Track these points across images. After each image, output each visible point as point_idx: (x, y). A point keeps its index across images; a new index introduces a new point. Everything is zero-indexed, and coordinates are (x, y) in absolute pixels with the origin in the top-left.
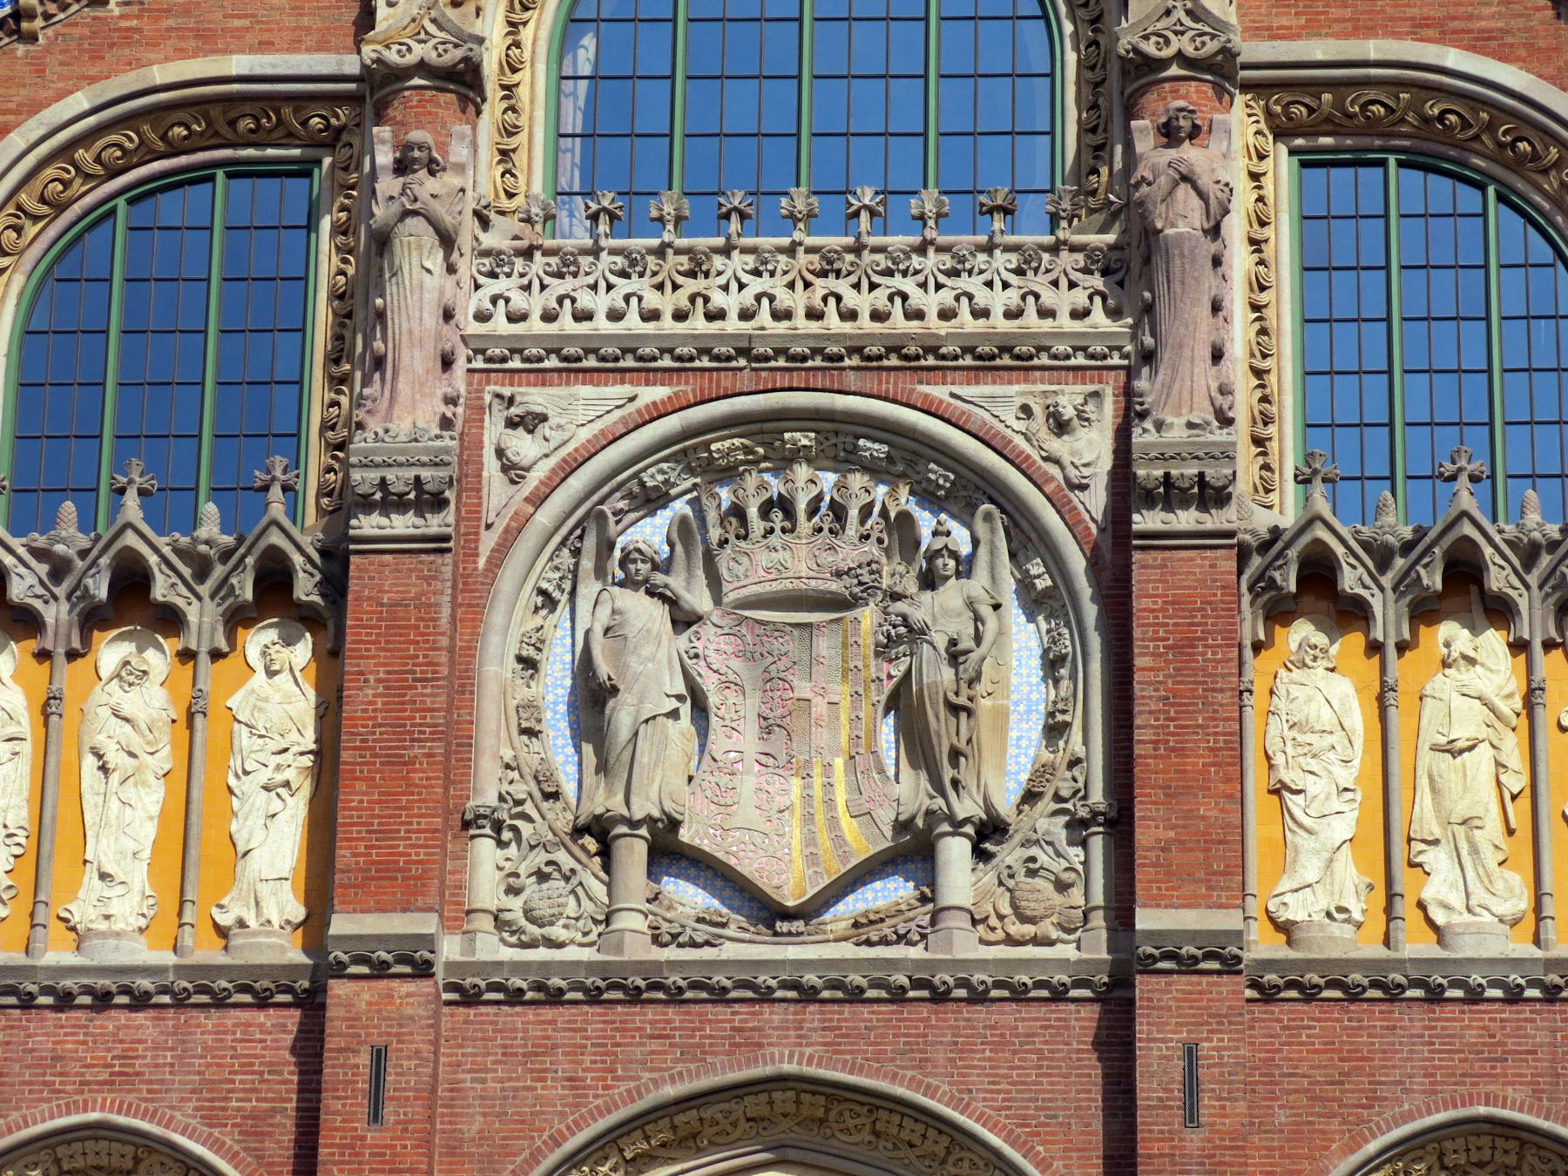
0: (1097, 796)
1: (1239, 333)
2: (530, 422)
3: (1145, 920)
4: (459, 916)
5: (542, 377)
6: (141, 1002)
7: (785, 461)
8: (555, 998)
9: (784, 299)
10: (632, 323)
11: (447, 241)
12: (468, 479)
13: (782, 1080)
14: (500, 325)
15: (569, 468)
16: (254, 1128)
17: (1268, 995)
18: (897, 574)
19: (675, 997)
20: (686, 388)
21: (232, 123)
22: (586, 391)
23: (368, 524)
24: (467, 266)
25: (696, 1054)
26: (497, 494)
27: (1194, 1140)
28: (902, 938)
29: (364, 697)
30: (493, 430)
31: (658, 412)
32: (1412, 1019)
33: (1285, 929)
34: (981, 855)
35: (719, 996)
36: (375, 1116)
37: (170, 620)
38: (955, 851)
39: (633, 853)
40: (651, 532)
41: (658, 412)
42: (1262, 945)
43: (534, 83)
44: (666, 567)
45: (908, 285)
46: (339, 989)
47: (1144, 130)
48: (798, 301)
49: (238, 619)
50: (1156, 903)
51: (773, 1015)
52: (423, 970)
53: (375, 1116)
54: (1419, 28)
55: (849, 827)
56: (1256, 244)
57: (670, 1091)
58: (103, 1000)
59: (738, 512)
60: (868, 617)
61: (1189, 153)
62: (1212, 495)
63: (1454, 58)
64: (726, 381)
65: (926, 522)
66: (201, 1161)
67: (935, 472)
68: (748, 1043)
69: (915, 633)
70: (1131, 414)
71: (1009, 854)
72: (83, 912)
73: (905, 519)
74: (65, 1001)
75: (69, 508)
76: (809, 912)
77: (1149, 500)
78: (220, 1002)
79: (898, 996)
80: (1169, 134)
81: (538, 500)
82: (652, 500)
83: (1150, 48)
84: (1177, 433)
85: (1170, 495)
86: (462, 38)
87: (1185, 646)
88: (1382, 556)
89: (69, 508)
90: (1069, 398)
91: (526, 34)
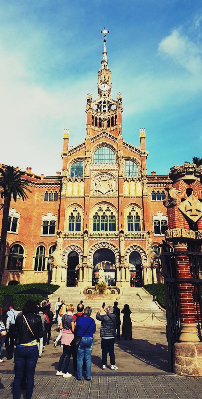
0: (117, 189)
1: (123, 169)
3: (119, 195)
4: (90, 194)
6: (77, 198)
7: (104, 174)
8: (94, 198)
10: (97, 168)
11: (89, 165)
12: (90, 175)
14: (91, 168)
15: (95, 175)
16: (82, 203)
17: (124, 198)
18: (109, 179)
19: (99, 198)
20: (99, 171)
23: (86, 177)
24: (90, 166)
25: (100, 200)
26: (91, 176)
27: (121, 204)
29: (86, 185)
30: (91, 173)
31: (98, 172)
32: (130, 199)
33: (125, 195)
35: (101, 198)
36: (87, 203)
37: (78, 181)
38: (111, 191)
39: (97, 191)
40: (98, 177)
41: (98, 172)
42: (124, 196)
43: (92, 157)
44: (98, 179)
46: (85, 198)
47: (119, 160)
48: (104, 167)
51: (103, 199)
52: (89, 197)
53: (87, 203)
54: (131, 155)
58: (75, 198)
59: (102, 177)
60: (107, 181)
61: (121, 161)
62: (122, 176)
63: (132, 157)
65: (110, 177)
68: (102, 200)
69: (109, 182)
70: (118, 173)
71: (113, 192)
72: (74, 194)
73: (109, 177)
74: (74, 198)
75: (73, 177)
76: (105, 194)
77: (119, 176)
78: (80, 198)
79: (109, 198)
80: (120, 160)
82: (98, 176)
84: (120, 174)
85: (120, 176)
87: (121, 183)
88: (129, 179)
89: (73, 177)
90: (116, 172)
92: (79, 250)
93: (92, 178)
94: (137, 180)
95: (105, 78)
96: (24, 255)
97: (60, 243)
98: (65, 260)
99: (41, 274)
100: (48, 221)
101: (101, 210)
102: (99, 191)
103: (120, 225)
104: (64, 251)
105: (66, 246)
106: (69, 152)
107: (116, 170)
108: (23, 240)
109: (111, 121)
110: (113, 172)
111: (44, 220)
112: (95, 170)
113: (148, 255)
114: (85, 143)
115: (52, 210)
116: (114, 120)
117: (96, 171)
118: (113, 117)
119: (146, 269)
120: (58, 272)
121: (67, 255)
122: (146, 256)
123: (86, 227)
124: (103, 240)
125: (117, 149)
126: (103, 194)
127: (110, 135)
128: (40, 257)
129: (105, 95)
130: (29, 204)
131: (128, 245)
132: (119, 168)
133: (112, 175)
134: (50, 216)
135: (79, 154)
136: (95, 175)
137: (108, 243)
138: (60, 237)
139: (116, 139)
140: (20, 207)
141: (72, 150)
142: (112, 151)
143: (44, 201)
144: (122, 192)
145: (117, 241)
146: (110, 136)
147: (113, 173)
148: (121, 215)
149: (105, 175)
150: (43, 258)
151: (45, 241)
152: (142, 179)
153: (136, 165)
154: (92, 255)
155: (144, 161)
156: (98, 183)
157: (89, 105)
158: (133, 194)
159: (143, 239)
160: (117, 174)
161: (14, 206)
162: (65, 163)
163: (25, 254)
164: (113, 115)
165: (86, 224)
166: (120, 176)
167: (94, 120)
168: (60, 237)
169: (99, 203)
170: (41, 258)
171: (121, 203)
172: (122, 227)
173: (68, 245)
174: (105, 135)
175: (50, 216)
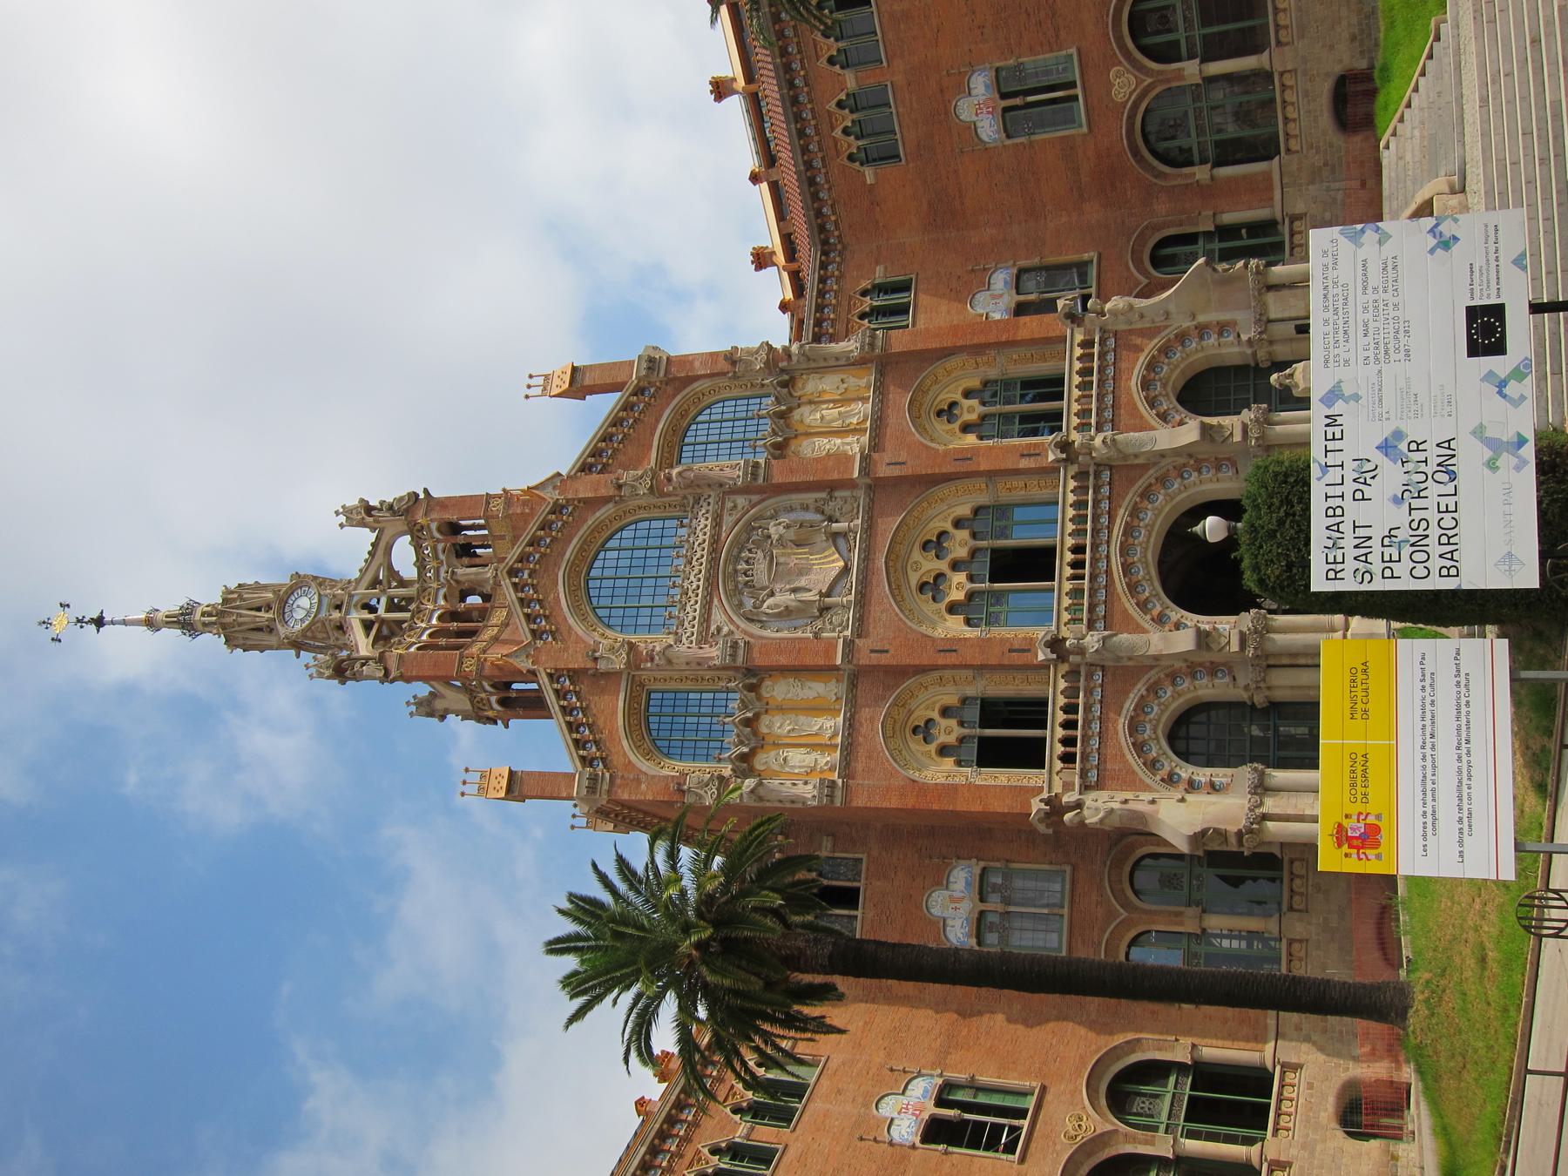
0: (824, 495)
2: (719, 630)
5: (708, 627)
9: (696, 571)
10: (697, 607)
22: (713, 617)
27: (909, 463)
28: (855, 538)
34: (837, 522)
36: (887, 651)
40: (749, 603)
45: (697, 544)
49: (759, 698)
50: (852, 473)
53: (887, 651)
57: (887, 588)
63: (660, 426)
64: (715, 584)
67: (743, 537)
72: (829, 733)
81: (738, 627)
83: (648, 486)
86: (623, 645)
90: (729, 505)
92: (1161, 693)
94: (785, 391)
95: (259, 609)
97: (1116, 806)
98: (1217, 776)
99: (1302, 954)
101: (933, 586)
102: (828, 594)
103: (1024, 463)
104: (1163, 780)
105: (1134, 772)
106: (584, 766)
107: (722, 501)
108: (1081, 1057)
110: (728, 520)
111: (973, 942)
112: (706, 618)
113: (1194, 316)
114: (550, 676)
117: (714, 610)
119: (1270, 321)
120: (1290, 811)
121: (1186, 771)
122: (1202, 330)
124: (1108, 557)
125: (611, 505)
126: (846, 570)
127: (530, 544)
129: (338, 607)
131: (1142, 417)
132: (709, 486)
133: (749, 529)
134: (953, 900)
136: (735, 618)
137: (1129, 531)
138: (1079, 805)
139: (557, 509)
140: (874, 1070)
142: (618, 536)
144: (843, 459)
145: (1116, 477)
146: (535, 542)
147: (734, 518)
149: (742, 566)
152: (783, 371)
153: (708, 411)
154: (1192, 619)
155: (691, 363)
156: (783, 599)
157: (363, 665)
158: (861, 411)
159: (1111, 343)
160: (741, 501)
161: (860, 1100)
162: (643, 786)
166: (755, 476)
167: (443, 641)
168: (1079, 805)
169: (896, 592)
172: (1039, 455)
173: (1129, 757)
175: (953, 900)
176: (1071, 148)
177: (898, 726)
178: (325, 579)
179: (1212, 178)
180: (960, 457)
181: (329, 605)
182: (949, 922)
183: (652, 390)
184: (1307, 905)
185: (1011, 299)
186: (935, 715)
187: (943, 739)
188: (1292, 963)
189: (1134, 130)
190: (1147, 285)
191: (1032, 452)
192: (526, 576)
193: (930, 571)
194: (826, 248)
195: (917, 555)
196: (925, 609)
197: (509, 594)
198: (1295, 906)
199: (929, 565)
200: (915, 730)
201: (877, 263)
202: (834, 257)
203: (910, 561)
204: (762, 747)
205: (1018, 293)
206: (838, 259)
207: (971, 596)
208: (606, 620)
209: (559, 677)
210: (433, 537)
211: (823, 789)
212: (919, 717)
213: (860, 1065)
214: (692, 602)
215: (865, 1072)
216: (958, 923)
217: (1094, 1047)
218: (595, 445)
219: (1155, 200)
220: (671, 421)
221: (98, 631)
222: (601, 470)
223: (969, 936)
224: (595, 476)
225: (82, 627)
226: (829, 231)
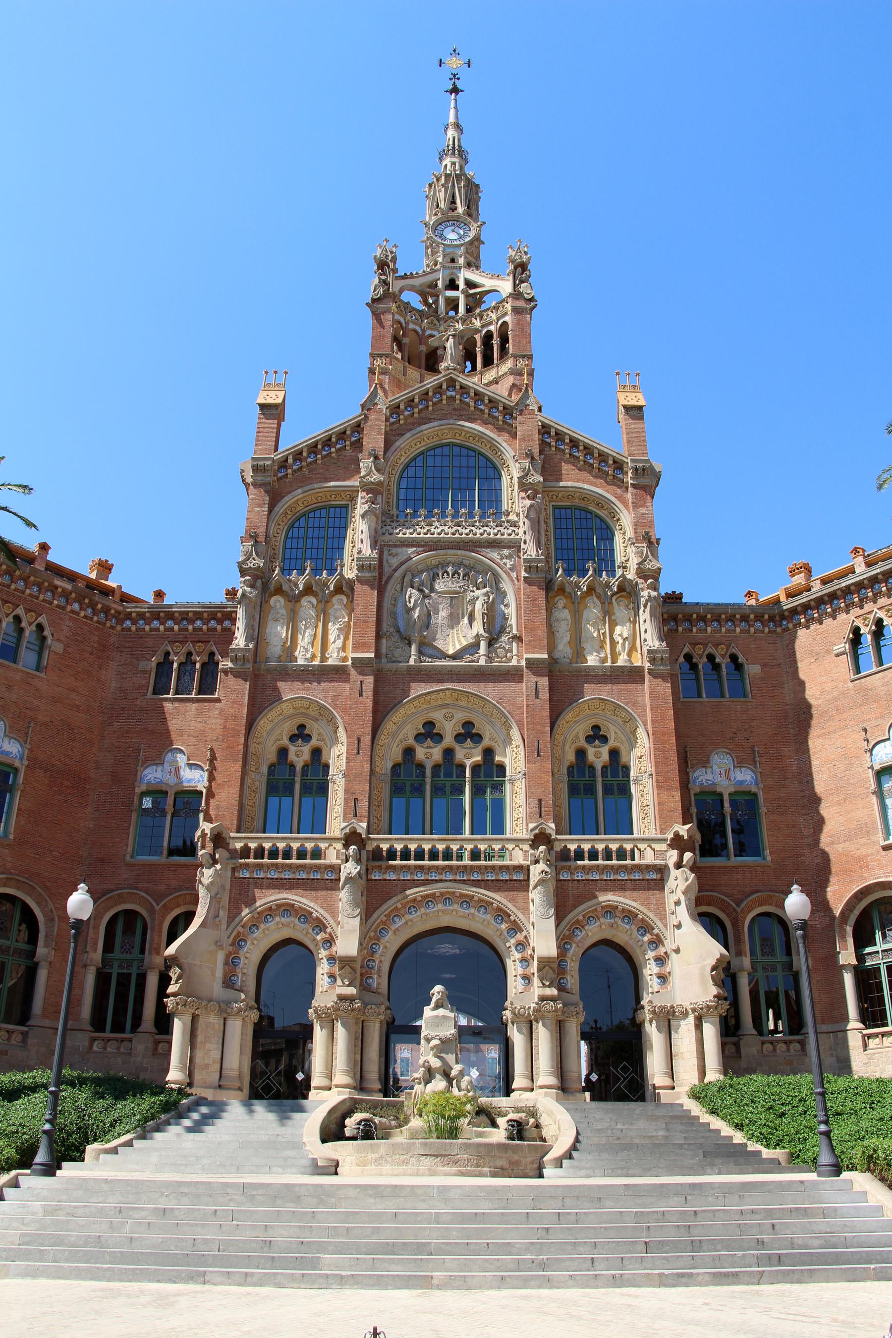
0: (514, 631)
13: (448, 689)
15: (402, 564)
21: (331, 496)
27: (538, 701)
36: (361, 695)
53: (361, 695)
55: (463, 640)
56: (546, 522)
63: (586, 486)
66: (323, 705)
81: (395, 570)
91: (392, 480)
93: (390, 578)
96: (41, 950)
99: (122, 1049)
100: (167, 793)
109: (479, 350)
111: (144, 788)
113: (677, 951)
114: (358, 425)
115: (185, 737)
116: (496, 342)
118: (489, 336)
123: (355, 815)
128: (120, 966)
130: (78, 707)
135: (328, 470)
141: (298, 455)
142: (489, 464)
143: (149, 694)
148: (539, 755)
150: (134, 972)
151: (145, 885)
162: (257, 509)
163: (46, 945)
164: (490, 323)
165: (356, 800)
170: (125, 971)
171: (537, 697)
172: (540, 816)
174: (453, 393)
176: (868, 832)
177: (304, 711)
178: (478, 248)
179: (843, 967)
180: (541, 746)
181: (453, 253)
182: (160, 768)
183: (621, 476)
184: (160, 1054)
185: (725, 787)
186: (314, 742)
187: (292, 749)
188: (115, 1042)
189: (885, 889)
190: (735, 910)
191: (543, 809)
192: (449, 393)
193: (444, 728)
194: (777, 618)
195: (461, 716)
196: (409, 726)
197: (431, 381)
198: (161, 1045)
199: (449, 729)
200: (302, 727)
201: (764, 666)
202: (768, 626)
203: (454, 711)
204: (290, 601)
205: (730, 794)
206: (766, 630)
207: (421, 766)
208: (413, 464)
209: (358, 432)
210: (498, 320)
211: (242, 651)
212: (313, 728)
213: (35, 702)
214: (419, 530)
215: (28, 707)
216: (159, 775)
217: (49, 884)
218: (566, 434)
219: (823, 914)
220: (576, 492)
221: (447, 91)
222: (546, 442)
223: (149, 783)
224: (536, 437)
225: (450, 79)
226: (792, 619)
